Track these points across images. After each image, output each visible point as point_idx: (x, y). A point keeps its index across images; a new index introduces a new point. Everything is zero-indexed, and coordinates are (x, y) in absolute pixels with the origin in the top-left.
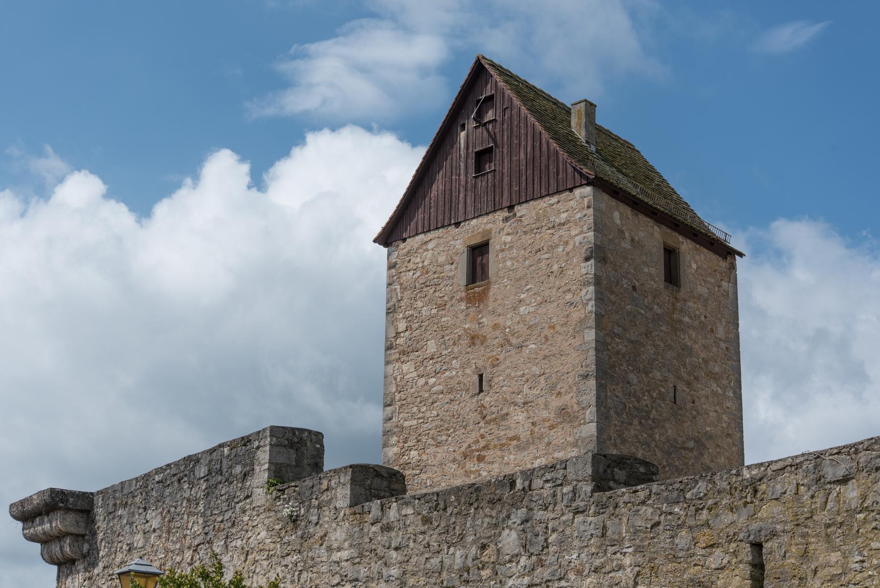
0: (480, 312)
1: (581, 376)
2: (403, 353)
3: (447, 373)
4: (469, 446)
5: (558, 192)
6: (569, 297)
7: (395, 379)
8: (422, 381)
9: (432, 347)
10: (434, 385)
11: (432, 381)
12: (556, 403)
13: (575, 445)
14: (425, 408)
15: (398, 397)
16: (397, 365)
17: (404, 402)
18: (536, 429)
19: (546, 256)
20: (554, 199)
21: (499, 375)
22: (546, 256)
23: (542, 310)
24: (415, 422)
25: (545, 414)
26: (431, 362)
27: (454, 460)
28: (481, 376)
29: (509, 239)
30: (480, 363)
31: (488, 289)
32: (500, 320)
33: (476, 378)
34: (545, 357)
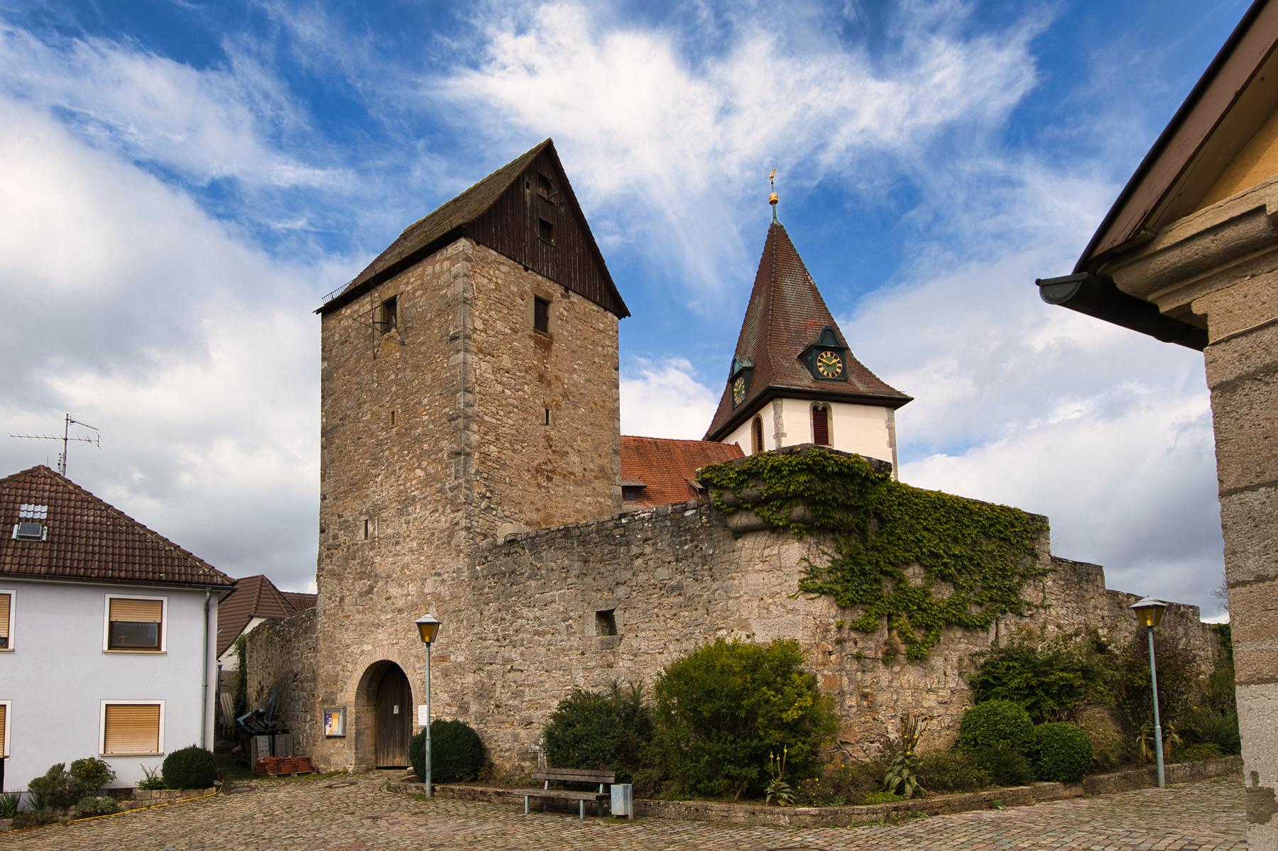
0: (545, 358)
1: (613, 449)
2: (481, 351)
3: (521, 393)
4: (540, 465)
5: (599, 304)
6: (605, 387)
7: (475, 371)
8: (500, 388)
9: (506, 362)
10: (509, 397)
11: (508, 392)
12: (598, 461)
13: (610, 497)
14: (502, 413)
15: (477, 389)
16: (476, 359)
17: (483, 397)
18: (586, 474)
19: (591, 347)
20: (595, 308)
21: (561, 419)
22: (591, 347)
23: (589, 386)
24: (494, 421)
25: (592, 466)
26: (506, 374)
27: (529, 471)
28: (547, 411)
29: (565, 313)
30: (548, 400)
31: (552, 343)
32: (560, 373)
33: (543, 410)
34: (591, 424)
